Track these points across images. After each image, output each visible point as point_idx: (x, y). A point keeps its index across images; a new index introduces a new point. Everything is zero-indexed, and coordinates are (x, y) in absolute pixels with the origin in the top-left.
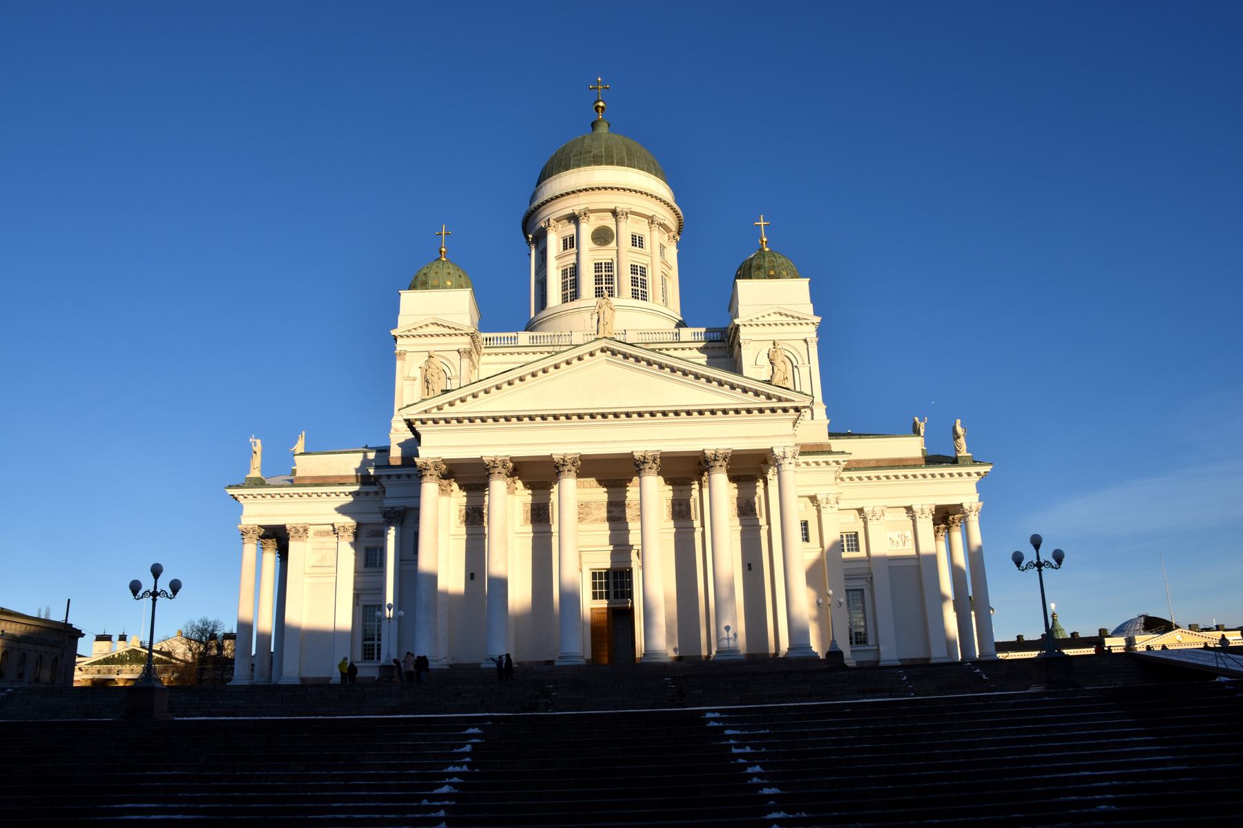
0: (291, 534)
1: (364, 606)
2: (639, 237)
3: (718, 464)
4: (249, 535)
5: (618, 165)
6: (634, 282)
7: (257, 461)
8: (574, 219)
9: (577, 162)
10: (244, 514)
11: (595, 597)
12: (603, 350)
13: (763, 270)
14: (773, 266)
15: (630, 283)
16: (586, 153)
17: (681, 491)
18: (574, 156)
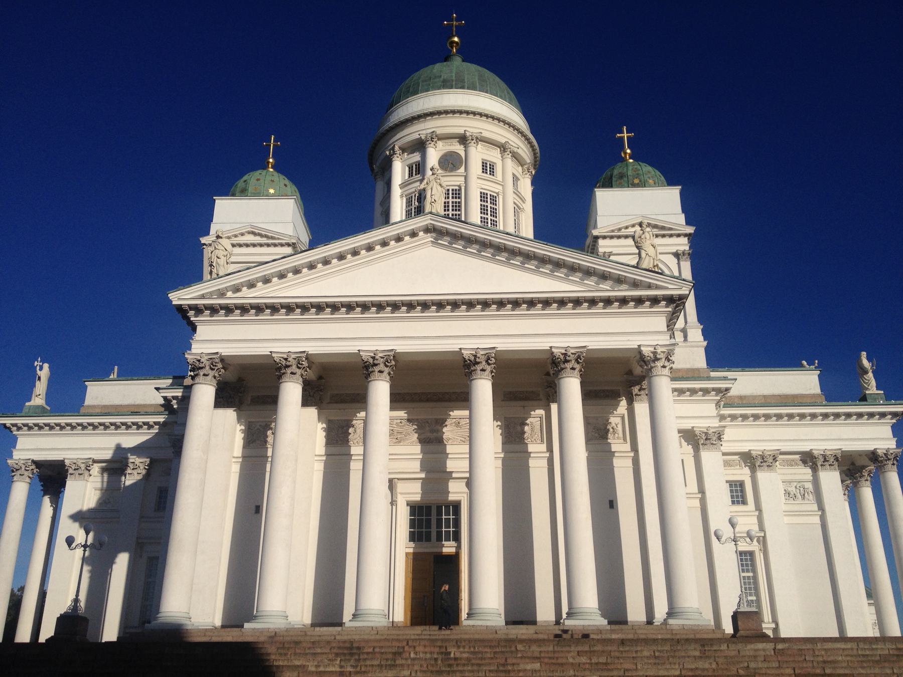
0: (71, 471)
2: (490, 165)
3: (569, 365)
4: (19, 472)
5: (468, 88)
6: (483, 210)
7: (41, 387)
9: (426, 87)
10: (17, 448)
12: (427, 230)
13: (626, 179)
14: (638, 174)
15: (479, 211)
16: (436, 77)
17: (524, 407)
18: (423, 81)
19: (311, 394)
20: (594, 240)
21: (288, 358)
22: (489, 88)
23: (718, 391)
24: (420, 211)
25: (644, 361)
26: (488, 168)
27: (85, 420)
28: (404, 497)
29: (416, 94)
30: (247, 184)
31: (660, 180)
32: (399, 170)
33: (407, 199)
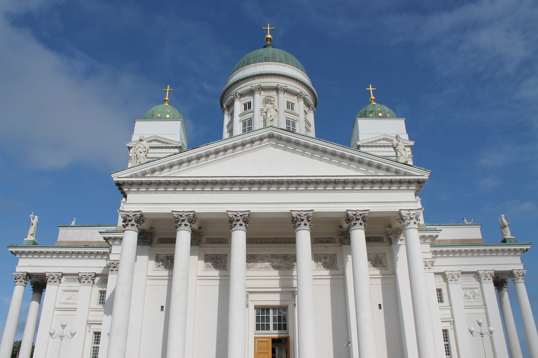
0: (49, 280)
1: (94, 332)
2: (291, 104)
4: (19, 280)
5: (279, 62)
7: (32, 230)
8: (251, 92)
10: (18, 265)
11: (258, 328)
19: (195, 237)
20: (358, 147)
21: (182, 215)
22: (290, 62)
23: (430, 236)
24: (250, 129)
25: (402, 219)
26: (290, 106)
27: (57, 250)
28: (253, 303)
29: (249, 65)
30: (154, 112)
31: (393, 115)
32: (238, 107)
33: (243, 123)
